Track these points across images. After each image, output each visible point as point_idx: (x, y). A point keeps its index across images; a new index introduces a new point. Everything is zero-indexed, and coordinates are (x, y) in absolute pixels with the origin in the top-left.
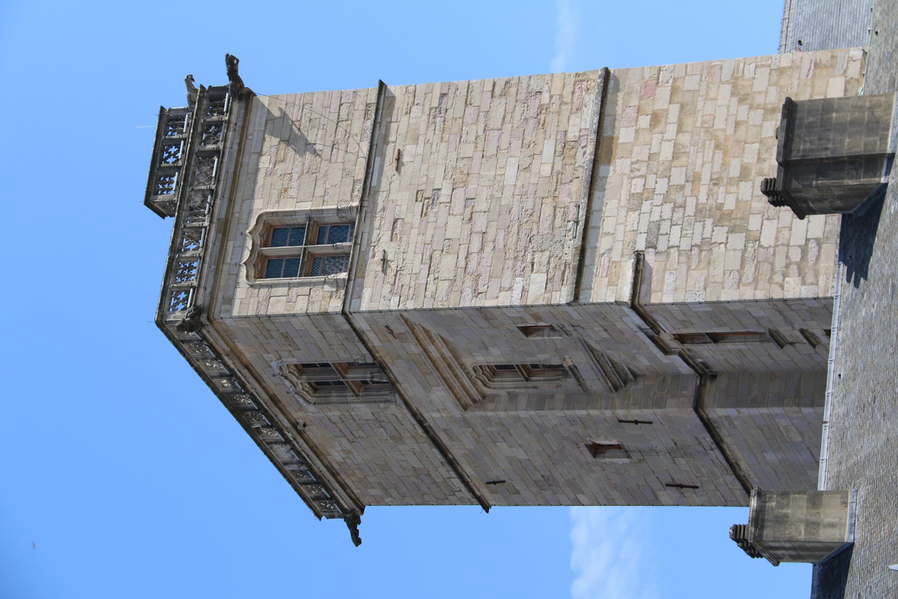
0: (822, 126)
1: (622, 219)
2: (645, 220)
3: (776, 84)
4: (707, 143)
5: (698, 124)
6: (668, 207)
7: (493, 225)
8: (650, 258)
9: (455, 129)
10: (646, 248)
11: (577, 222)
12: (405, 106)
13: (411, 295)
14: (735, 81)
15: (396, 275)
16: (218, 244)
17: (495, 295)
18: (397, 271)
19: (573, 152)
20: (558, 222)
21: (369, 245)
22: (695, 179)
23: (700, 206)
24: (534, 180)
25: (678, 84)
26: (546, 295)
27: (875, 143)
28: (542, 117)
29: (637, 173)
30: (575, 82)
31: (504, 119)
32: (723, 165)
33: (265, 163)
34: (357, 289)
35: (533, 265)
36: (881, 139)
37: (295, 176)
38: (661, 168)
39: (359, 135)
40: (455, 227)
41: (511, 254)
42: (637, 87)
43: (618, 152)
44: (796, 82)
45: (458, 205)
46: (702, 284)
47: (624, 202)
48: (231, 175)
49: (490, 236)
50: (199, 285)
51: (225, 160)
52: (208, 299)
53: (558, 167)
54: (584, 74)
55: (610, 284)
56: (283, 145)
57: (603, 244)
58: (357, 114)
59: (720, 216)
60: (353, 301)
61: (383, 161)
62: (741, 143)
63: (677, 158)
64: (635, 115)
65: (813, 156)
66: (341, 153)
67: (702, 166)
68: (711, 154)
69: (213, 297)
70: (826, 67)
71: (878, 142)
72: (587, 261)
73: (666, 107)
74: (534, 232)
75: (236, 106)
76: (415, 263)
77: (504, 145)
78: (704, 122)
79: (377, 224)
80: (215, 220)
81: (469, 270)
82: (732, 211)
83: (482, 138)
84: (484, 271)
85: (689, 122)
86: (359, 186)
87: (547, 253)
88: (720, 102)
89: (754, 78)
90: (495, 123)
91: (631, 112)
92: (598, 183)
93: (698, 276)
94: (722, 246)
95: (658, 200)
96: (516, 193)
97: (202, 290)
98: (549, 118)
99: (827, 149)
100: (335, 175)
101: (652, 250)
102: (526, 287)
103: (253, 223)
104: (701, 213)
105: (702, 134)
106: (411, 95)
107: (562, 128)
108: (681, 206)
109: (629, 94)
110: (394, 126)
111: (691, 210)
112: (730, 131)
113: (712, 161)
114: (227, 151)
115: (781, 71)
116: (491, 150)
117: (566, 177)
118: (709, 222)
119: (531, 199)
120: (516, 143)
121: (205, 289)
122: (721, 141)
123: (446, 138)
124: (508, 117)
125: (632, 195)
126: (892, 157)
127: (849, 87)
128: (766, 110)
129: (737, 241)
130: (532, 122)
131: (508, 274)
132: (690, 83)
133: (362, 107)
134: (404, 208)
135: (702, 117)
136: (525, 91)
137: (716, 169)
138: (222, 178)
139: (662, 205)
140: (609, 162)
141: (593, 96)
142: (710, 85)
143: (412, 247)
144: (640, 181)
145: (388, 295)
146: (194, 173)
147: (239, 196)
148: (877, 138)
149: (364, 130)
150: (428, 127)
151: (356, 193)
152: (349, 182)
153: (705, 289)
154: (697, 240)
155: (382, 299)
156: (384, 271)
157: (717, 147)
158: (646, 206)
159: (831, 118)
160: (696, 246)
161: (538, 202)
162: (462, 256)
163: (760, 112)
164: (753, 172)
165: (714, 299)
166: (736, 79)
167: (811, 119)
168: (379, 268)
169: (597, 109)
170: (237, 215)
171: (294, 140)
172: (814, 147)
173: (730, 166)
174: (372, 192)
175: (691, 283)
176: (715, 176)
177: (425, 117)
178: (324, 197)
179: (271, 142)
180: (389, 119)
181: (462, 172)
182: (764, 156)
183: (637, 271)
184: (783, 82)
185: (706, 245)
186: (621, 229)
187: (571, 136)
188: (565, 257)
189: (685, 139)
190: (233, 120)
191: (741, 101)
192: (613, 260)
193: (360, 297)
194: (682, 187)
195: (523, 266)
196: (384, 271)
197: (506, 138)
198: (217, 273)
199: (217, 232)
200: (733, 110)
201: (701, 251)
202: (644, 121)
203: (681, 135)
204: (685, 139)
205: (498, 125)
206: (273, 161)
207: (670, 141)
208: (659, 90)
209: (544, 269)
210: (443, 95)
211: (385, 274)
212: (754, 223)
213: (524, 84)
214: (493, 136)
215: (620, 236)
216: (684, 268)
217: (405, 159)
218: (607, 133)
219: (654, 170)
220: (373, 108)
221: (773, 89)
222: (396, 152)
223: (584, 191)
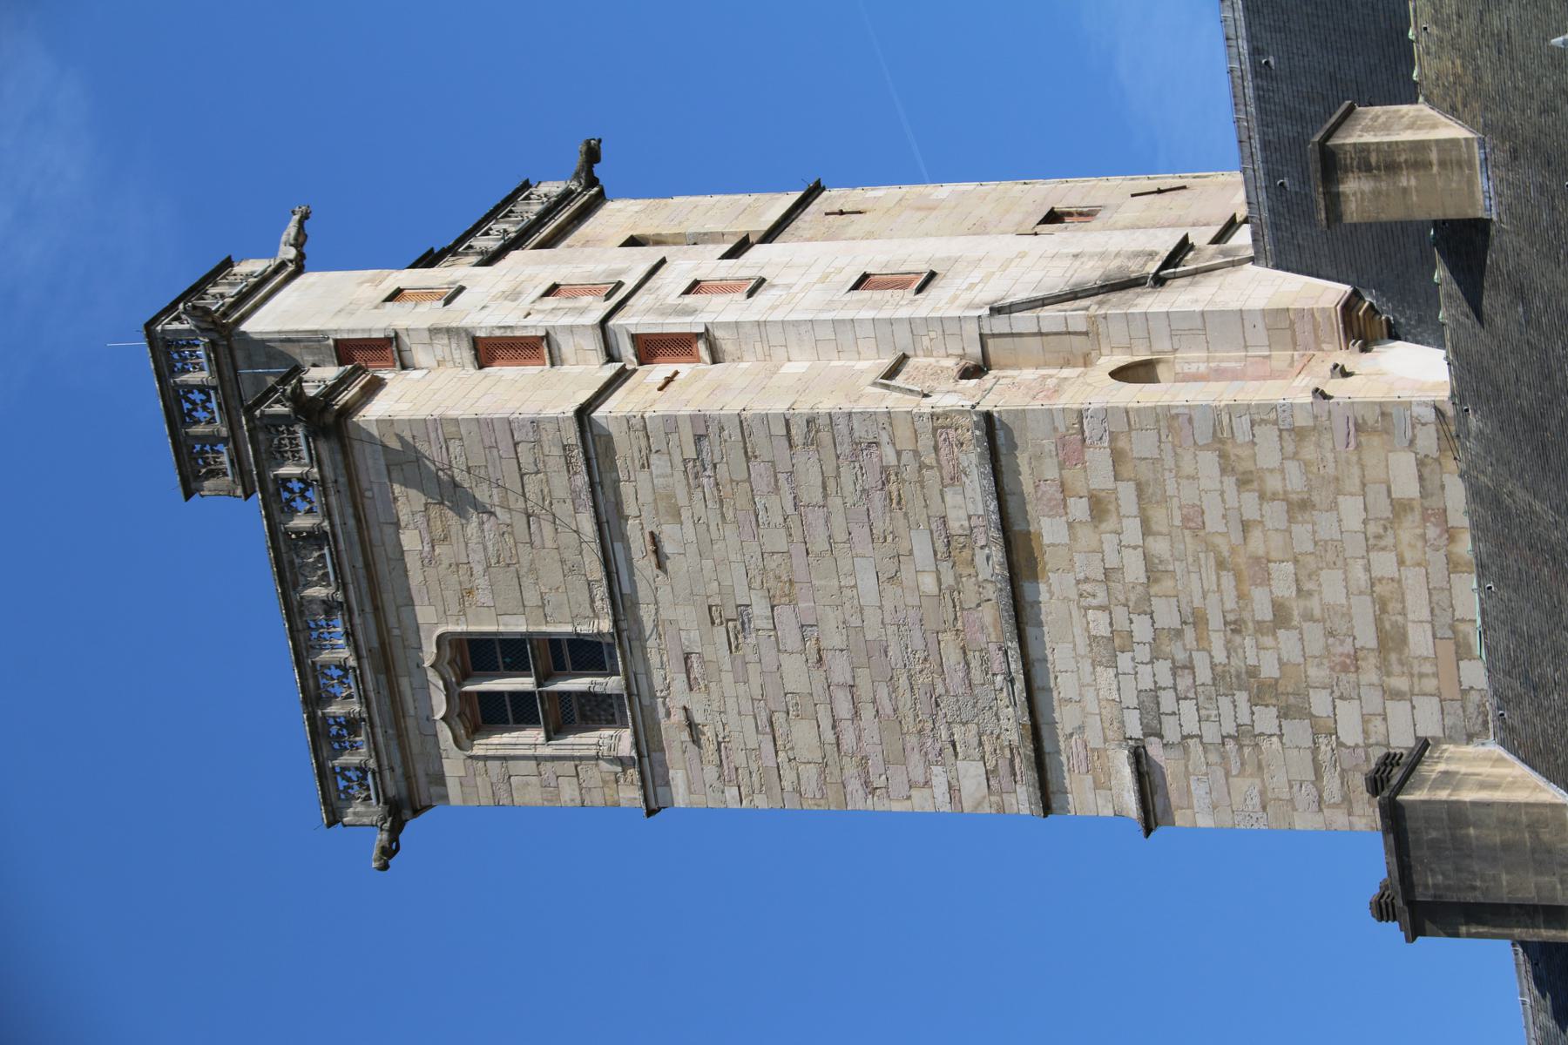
1: (1088, 679)
2: (1128, 684)
3: (1295, 456)
4: (1202, 555)
5: (1177, 522)
6: (1163, 667)
7: (863, 673)
8: (1154, 749)
9: (742, 502)
10: (1146, 735)
11: (1012, 681)
12: (636, 454)
13: (757, 786)
15: (719, 750)
16: (385, 692)
17: (905, 793)
18: (719, 744)
19: (966, 553)
20: (977, 676)
21: (653, 696)
22: (1198, 620)
23: (1219, 669)
24: (913, 600)
25: (1122, 443)
26: (993, 799)
27: (1554, 888)
28: (893, 487)
29: (1095, 602)
30: (935, 430)
31: (824, 488)
32: (1239, 597)
33: (410, 540)
34: (658, 770)
35: (954, 745)
37: (478, 569)
38: (1133, 597)
39: (569, 501)
40: (796, 673)
41: (909, 724)
42: (1049, 445)
43: (1050, 560)
44: (1330, 456)
45: (791, 639)
46: (1257, 800)
47: (1082, 649)
48: (362, 572)
49: (864, 691)
50: (380, 766)
51: (342, 546)
52: (402, 784)
53: (948, 579)
54: (946, 415)
55: (1097, 786)
56: (434, 511)
57: (1064, 718)
58: (551, 462)
59: (1262, 692)
60: (659, 790)
61: (628, 549)
63: (1157, 581)
64: (1059, 496)
65: (1453, 897)
66: (548, 529)
67: (1204, 598)
68: (1214, 578)
69: (408, 777)
70: (1375, 431)
72: (1047, 746)
74: (940, 689)
75: (324, 448)
76: (745, 733)
77: (840, 536)
78: (1185, 519)
79: (654, 659)
80: (364, 653)
81: (844, 748)
82: (1277, 680)
83: (796, 519)
84: (871, 746)
85: (1158, 516)
86: (601, 591)
87: (973, 728)
88: (1205, 483)
89: (1254, 444)
90: (813, 494)
91: (1052, 490)
92: (1028, 613)
93: (1246, 787)
94: (1275, 739)
95: (1143, 653)
96: (887, 621)
97: (387, 774)
98: (907, 491)
99: (1474, 888)
100: (552, 574)
101: (1152, 739)
102: (954, 782)
103: (429, 652)
104: (1219, 676)
105: (1188, 539)
106: (641, 434)
107: (936, 507)
108: (1184, 667)
109: (1038, 457)
110: (626, 489)
111: (1204, 675)
112: (1236, 537)
114: (339, 530)
115: (1300, 434)
116: (819, 544)
117: (969, 596)
118: (1242, 697)
119: (917, 634)
120: (861, 533)
121: (392, 769)
122: (1226, 554)
123: (730, 515)
124: (831, 484)
125: (1093, 639)
127: (1426, 472)
128: (1289, 503)
129: (1298, 731)
130: (877, 497)
131: (915, 758)
132: (1142, 445)
133: (557, 451)
134: (695, 635)
135: (1180, 508)
136: (847, 439)
137: (1230, 604)
138: (349, 578)
139: (1151, 662)
140: (1035, 577)
141: (974, 458)
142: (1179, 450)
143: (731, 703)
144: (1103, 617)
145: (717, 784)
146: (292, 563)
147: (387, 597)
148: (1555, 879)
149: (575, 494)
150: (690, 494)
151: (598, 604)
152: (580, 583)
153: (1264, 808)
154: (1229, 728)
155: (709, 791)
156: (696, 741)
157: (1221, 565)
158: (1124, 661)
159: (1468, 836)
160: (1229, 736)
161: (931, 638)
162: (826, 723)
163: (1279, 507)
164: (1296, 613)
166: (1222, 441)
167: (1434, 834)
168: (685, 736)
169: (989, 483)
170: (396, 632)
171: (452, 495)
174: (628, 604)
175: (1237, 799)
176: (1231, 617)
177: (679, 475)
178: (543, 606)
179: (409, 503)
180: (614, 475)
181: (778, 578)
182: (1308, 586)
184: (1309, 452)
185: (1243, 735)
186: (1090, 694)
187: (955, 526)
188: (1005, 737)
189: (1159, 546)
190: (329, 474)
191: (1244, 482)
192: (1091, 745)
193: (667, 784)
194: (1179, 633)
195: (938, 746)
196: (696, 741)
197: (838, 521)
198: (401, 736)
199: (376, 671)
200: (1232, 501)
201: (1241, 747)
205: (817, 497)
206: (427, 539)
207: (1135, 548)
208: (1089, 454)
209: (978, 756)
210: (698, 438)
211: (700, 747)
212: (1320, 703)
213: (842, 427)
214: (815, 517)
215: (1092, 707)
216: (1220, 773)
217: (668, 548)
218: (1018, 527)
219: (1122, 598)
220: (578, 454)
221: (1292, 466)
222: (648, 537)
223: (1009, 627)
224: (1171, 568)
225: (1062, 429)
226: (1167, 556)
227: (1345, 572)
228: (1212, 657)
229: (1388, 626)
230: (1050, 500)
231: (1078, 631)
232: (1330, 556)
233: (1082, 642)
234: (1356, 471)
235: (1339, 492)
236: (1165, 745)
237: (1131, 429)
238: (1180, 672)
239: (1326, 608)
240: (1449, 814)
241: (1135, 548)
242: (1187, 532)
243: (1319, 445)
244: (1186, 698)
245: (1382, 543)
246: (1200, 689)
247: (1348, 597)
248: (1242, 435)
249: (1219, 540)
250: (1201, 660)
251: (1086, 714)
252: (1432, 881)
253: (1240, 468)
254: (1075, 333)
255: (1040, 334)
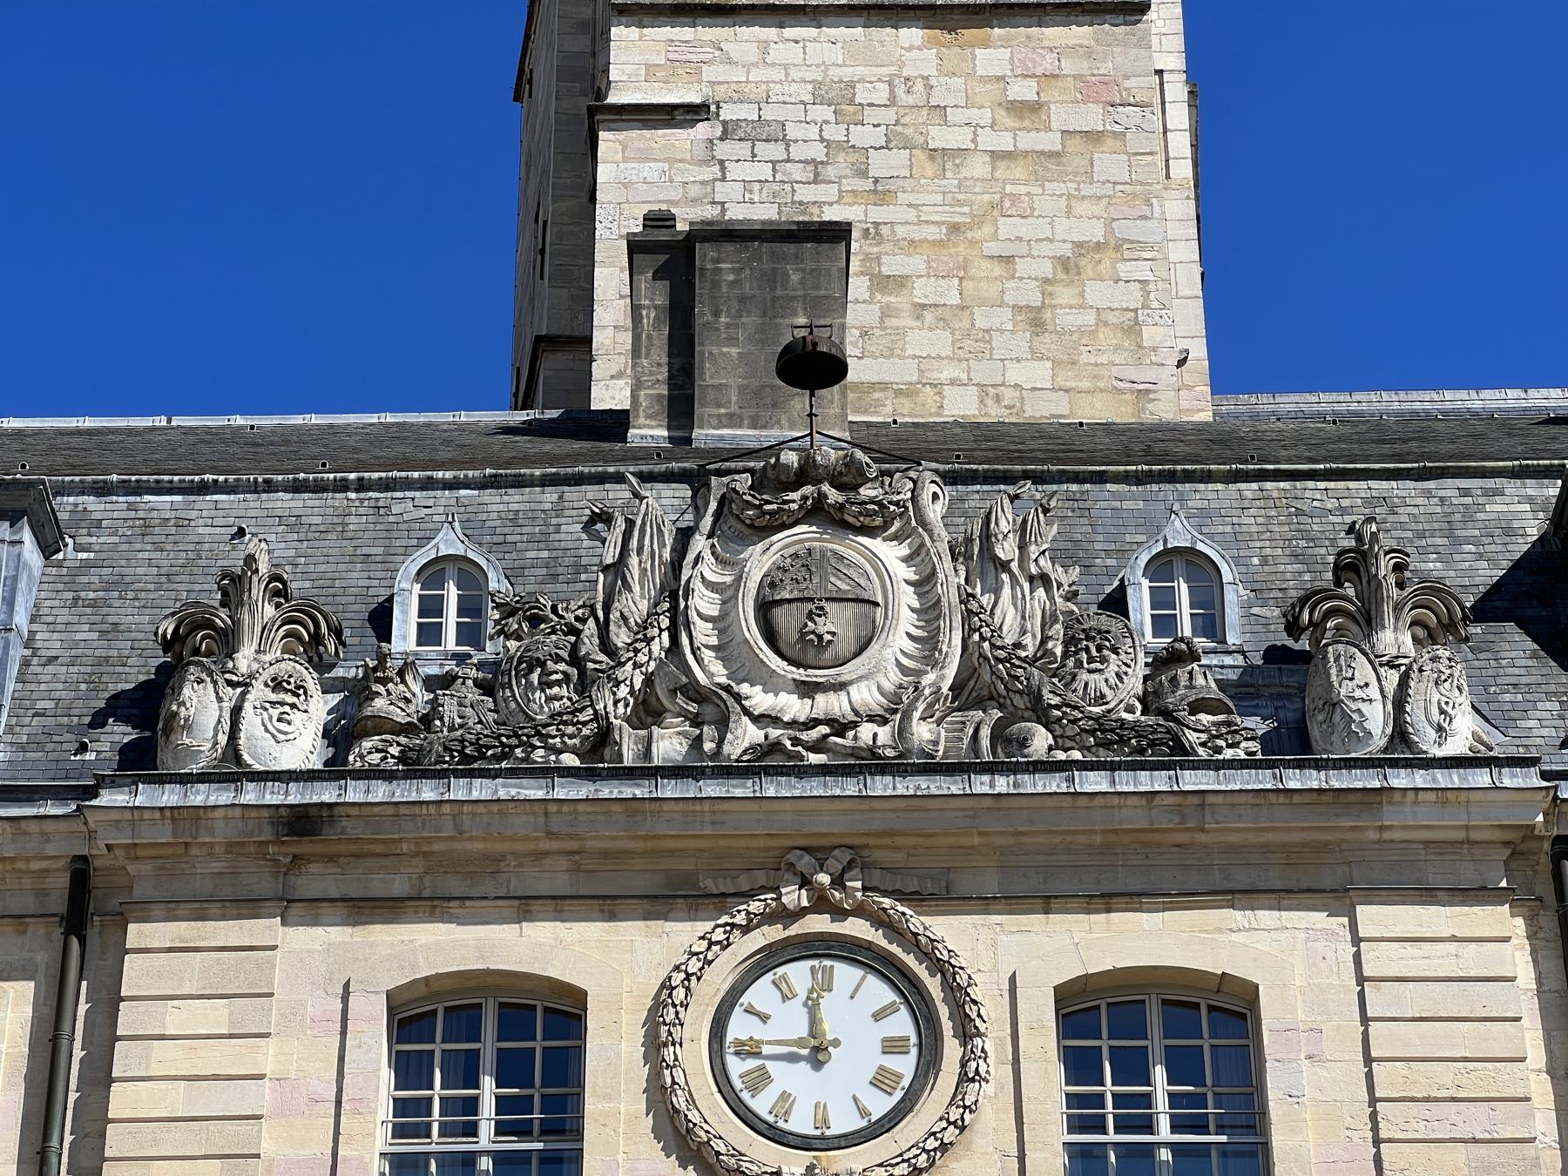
0: (774, 300)
1: (794, 74)
2: (792, 113)
4: (966, 209)
5: (1009, 189)
8: (702, 130)
10: (725, 123)
14: (1117, 246)
25: (1110, 142)
29: (900, 91)
32: (912, 242)
36: (730, 416)
38: (909, 131)
42: (1106, 68)
44: (1104, 359)
47: (835, 73)
62: (962, 272)
63: (932, 158)
64: (1039, 71)
67: (909, 205)
68: (937, 218)
71: (723, 411)
73: (1054, 125)
78: (1015, 198)
85: (1019, 171)
88: (1062, 225)
89: (1116, 281)
91: (1047, 64)
95: (835, 133)
99: (716, 314)
101: (719, 132)
105: (987, 197)
109: (1089, 54)
112: (991, 248)
113: (920, 222)
115: (1133, 329)
122: (969, 235)
126: (689, 441)
128: (1039, 310)
132: (1109, 164)
135: (1028, 194)
137: (901, 231)
139: (822, 140)
144: (882, 95)
148: (734, 408)
157: (955, 228)
158: (825, 113)
159: (795, 315)
160: (724, 211)
164: (892, 299)
165: (597, 257)
166: (1117, 248)
167: (795, 278)
172: (724, 289)
173: (909, 255)
176: (885, 230)
182: (929, 317)
183: (670, 109)
184: (1106, 337)
189: (978, 167)
191: (1064, 263)
192: (705, 67)
194: (863, 173)
202: (1024, 90)
203: (988, 159)
204: (978, 167)
207: (974, 141)
219: (907, 120)
221: (1090, 318)
224: (949, 174)
225: (1127, 84)
226: (964, 173)
227: (948, 357)
228: (831, 204)
229: (876, 395)
230: (1034, 61)
231: (860, 71)
232: (969, 344)
233: (847, 73)
234: (1086, 384)
235: (1056, 363)
236: (711, 141)
237: (1130, 155)
238: (811, 168)
239: (901, 333)
240: (826, 297)
241: (974, 141)
242: (997, 197)
243: (1117, 348)
244: (774, 169)
245: (989, 402)
246: (787, 187)
247: (915, 357)
248: (1124, 269)
249: (987, 229)
250: (827, 192)
251: (748, 67)
252: (722, 267)
253: (1083, 262)
254: (1167, 167)
255: (1165, 131)
